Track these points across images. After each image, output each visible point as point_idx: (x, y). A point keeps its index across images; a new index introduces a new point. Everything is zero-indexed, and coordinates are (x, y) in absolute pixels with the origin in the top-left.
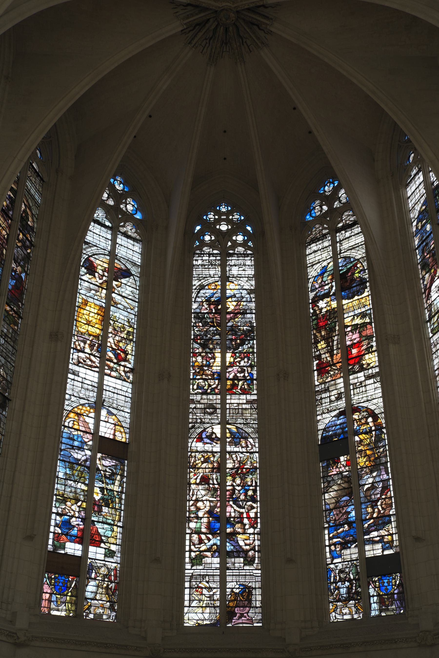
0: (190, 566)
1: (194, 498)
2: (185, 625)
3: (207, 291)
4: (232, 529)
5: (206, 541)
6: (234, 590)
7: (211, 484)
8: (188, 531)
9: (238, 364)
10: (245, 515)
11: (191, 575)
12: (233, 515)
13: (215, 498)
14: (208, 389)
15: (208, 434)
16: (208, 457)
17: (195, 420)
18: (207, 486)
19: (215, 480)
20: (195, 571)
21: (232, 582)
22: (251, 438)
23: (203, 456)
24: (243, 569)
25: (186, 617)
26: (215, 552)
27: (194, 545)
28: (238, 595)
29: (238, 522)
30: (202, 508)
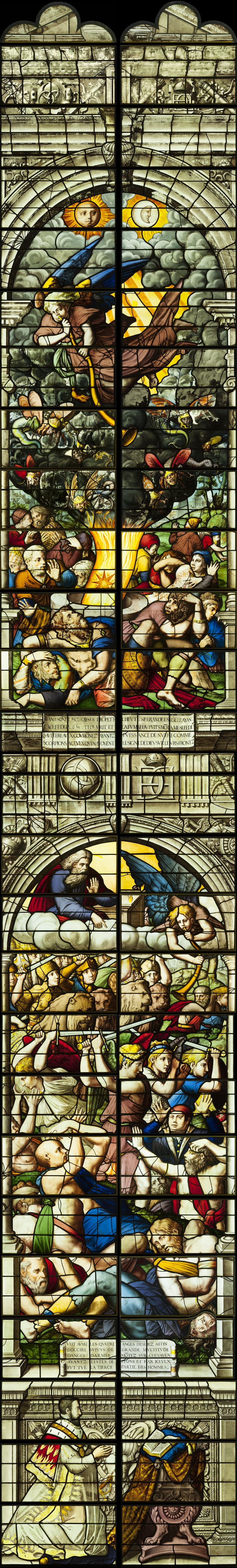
0: (19, 1369)
1: (26, 1127)
2: (5, 1561)
3: (64, 238)
4: (139, 1238)
5: (71, 1281)
6: (148, 1447)
7: (85, 1074)
8: (9, 1248)
9: (165, 580)
10: (184, 1188)
11: (20, 1397)
12: (143, 1185)
13: (101, 1125)
14: (70, 688)
15: (71, 879)
16: (74, 970)
17: (23, 823)
18: (70, 1081)
19: (99, 1060)
20: (35, 1384)
21: (142, 1420)
22: (210, 893)
23: (56, 968)
24: (176, 1379)
25: (8, 1539)
26: (100, 1318)
27: (30, 1293)
28: (162, 1463)
29: (161, 1215)
30: (53, 1162)
